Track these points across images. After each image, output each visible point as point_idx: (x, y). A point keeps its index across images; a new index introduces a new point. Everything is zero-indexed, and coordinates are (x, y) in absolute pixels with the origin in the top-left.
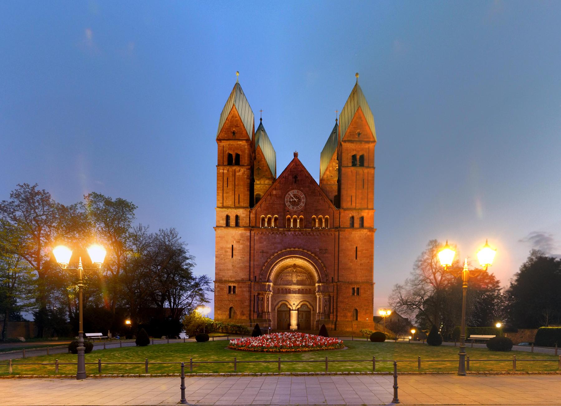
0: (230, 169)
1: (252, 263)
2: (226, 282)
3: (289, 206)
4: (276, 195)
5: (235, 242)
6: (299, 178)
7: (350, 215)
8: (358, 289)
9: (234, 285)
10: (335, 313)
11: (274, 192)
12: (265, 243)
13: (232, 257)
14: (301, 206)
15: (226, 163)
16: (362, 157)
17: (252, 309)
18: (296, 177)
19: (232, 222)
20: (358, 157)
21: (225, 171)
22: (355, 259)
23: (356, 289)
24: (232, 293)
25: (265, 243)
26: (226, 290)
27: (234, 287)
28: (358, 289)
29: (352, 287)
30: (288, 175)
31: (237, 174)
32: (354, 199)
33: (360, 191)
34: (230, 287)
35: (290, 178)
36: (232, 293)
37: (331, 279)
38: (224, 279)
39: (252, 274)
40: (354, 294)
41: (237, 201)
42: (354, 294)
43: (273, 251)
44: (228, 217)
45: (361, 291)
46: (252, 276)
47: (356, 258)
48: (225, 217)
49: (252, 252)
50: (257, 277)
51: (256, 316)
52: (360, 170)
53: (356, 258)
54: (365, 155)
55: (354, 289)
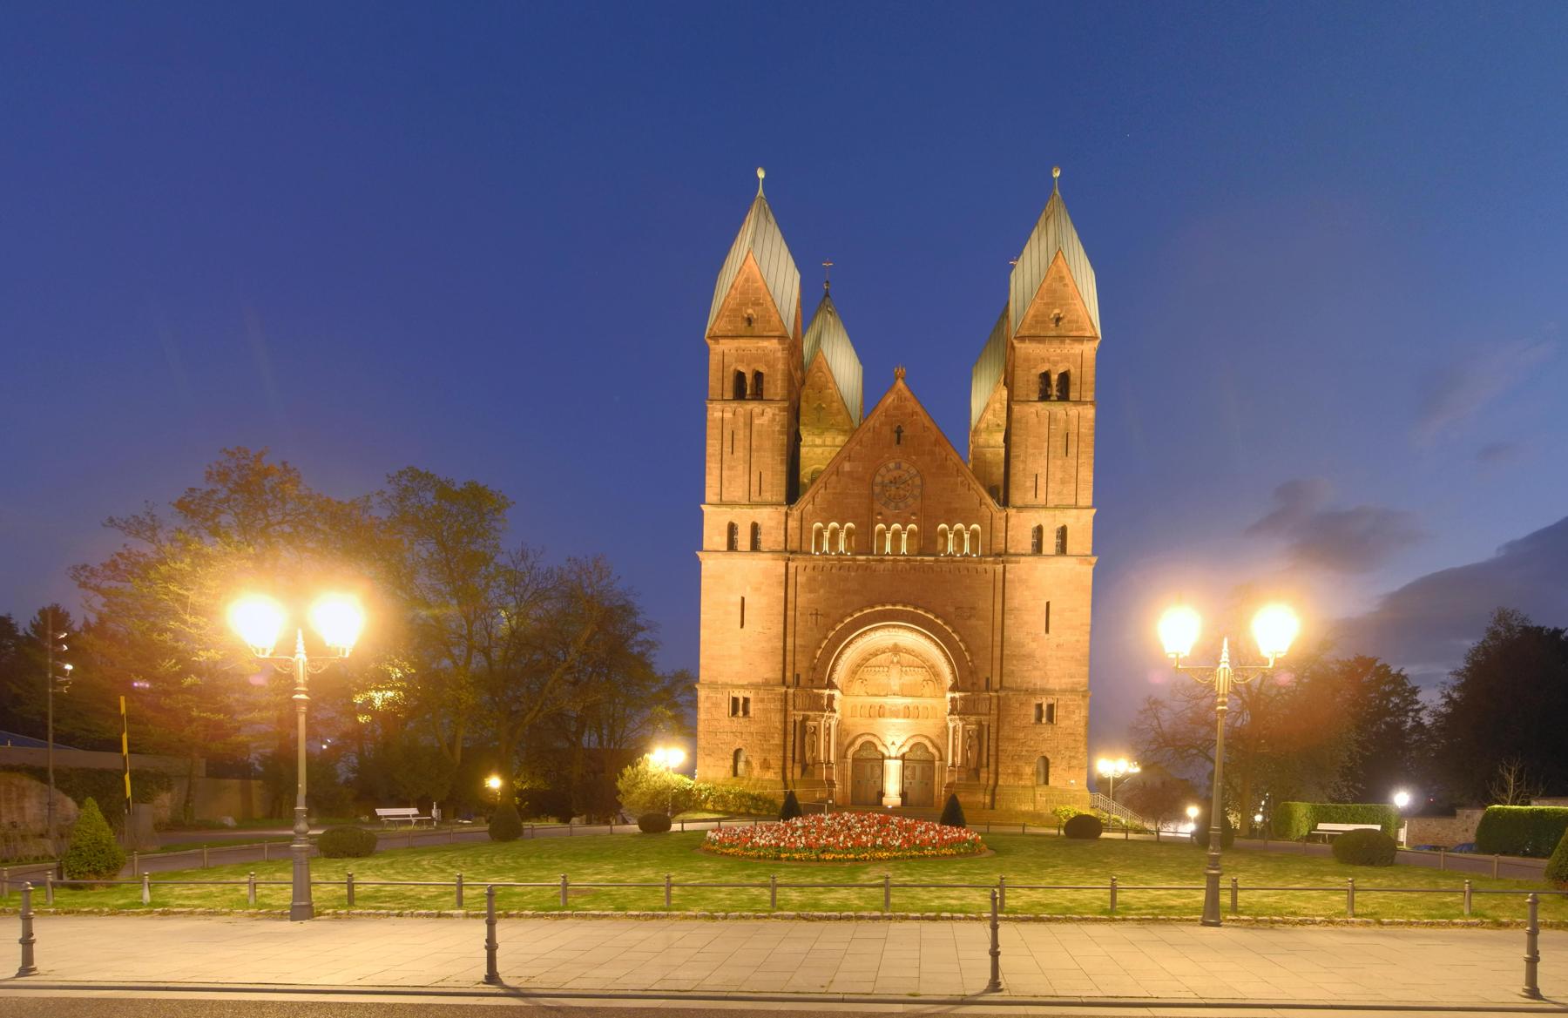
0: (740, 410)
1: (790, 640)
2: (725, 685)
4: (850, 474)
6: (906, 433)
7: (1035, 525)
8: (1051, 707)
10: (992, 767)
11: (847, 466)
15: (729, 395)
16: (1065, 378)
17: (790, 754)
18: (899, 431)
19: (744, 540)
20: (1054, 377)
21: (728, 415)
23: (1045, 707)
24: (741, 713)
26: (726, 707)
27: (746, 700)
28: (1051, 707)
29: (1035, 701)
30: (882, 424)
31: (757, 421)
32: (1042, 481)
33: (1059, 462)
34: (735, 700)
35: (886, 431)
36: (741, 713)
37: (983, 683)
38: (721, 680)
39: (789, 668)
40: (1039, 719)
41: (755, 488)
42: (1039, 719)
44: (732, 529)
45: (1059, 713)
46: (789, 674)
48: (725, 529)
49: (790, 613)
50: (803, 677)
51: (798, 771)
52: (1058, 409)
54: (1072, 371)
55: (1039, 706)
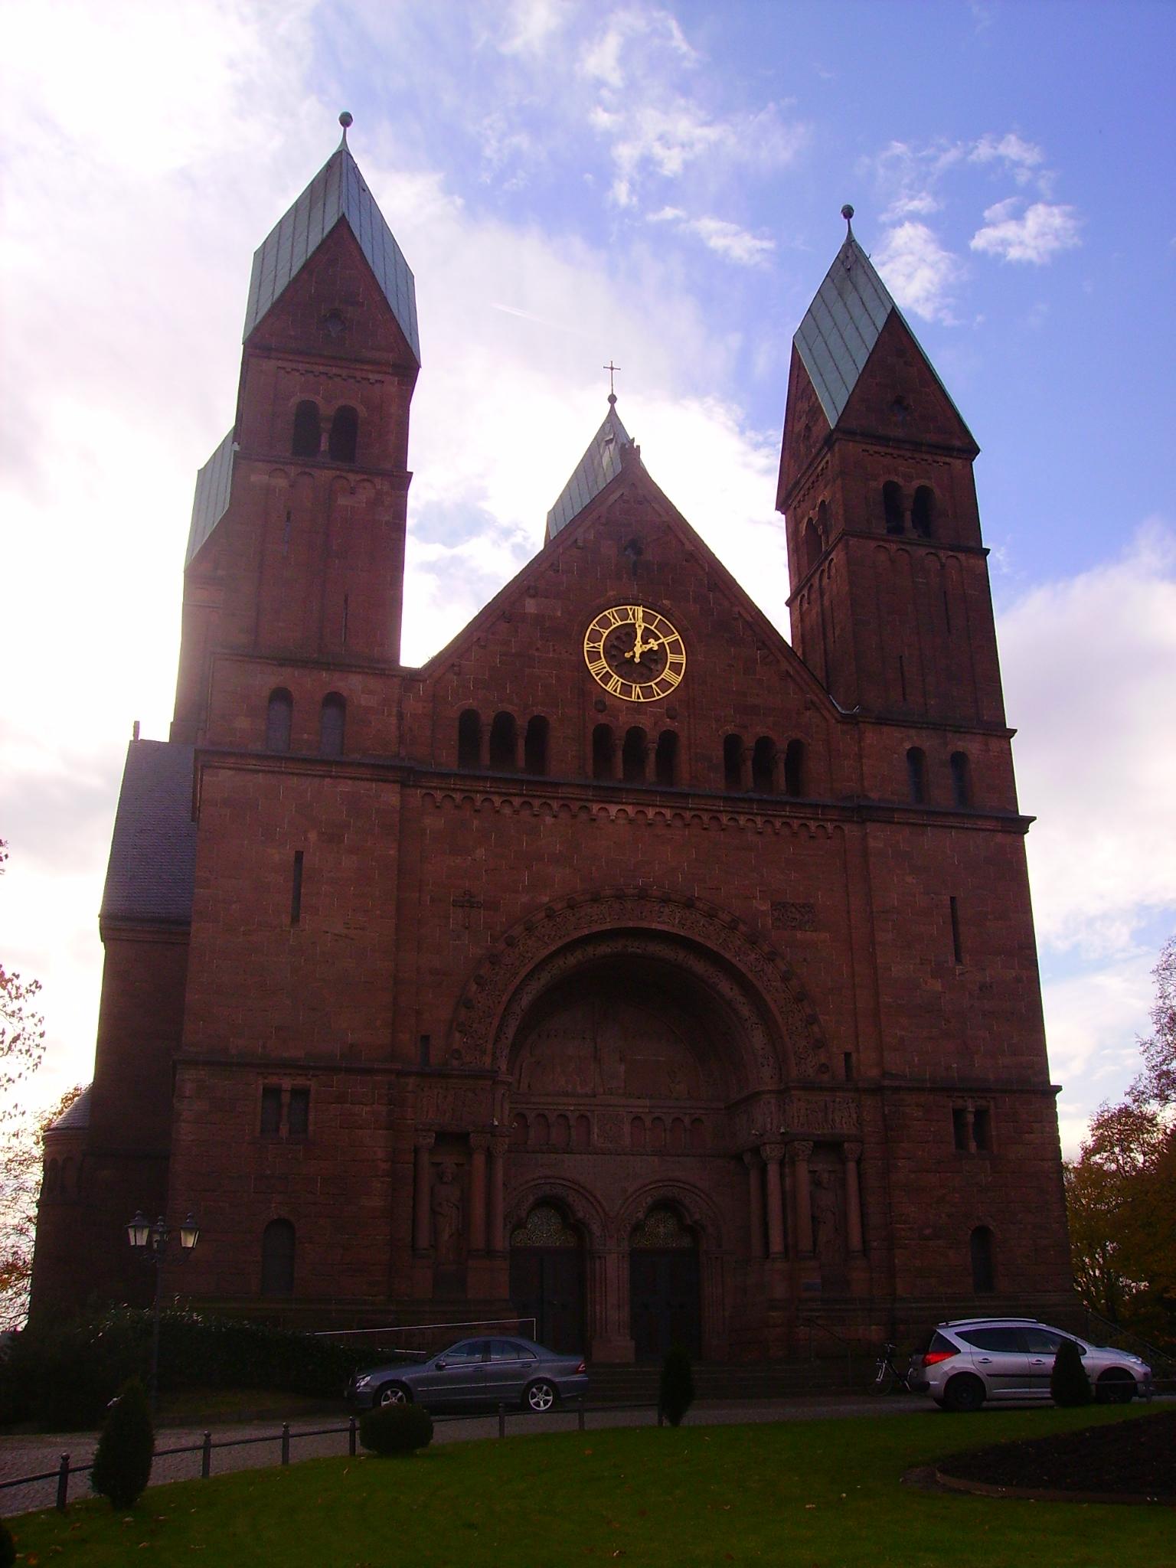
3: (606, 678)
7: (908, 746)
8: (981, 1114)
12: (480, 853)
13: (295, 919)
14: (664, 685)
22: (951, 959)
25: (480, 853)
27: (301, 1093)
28: (981, 1114)
37: (839, 1062)
40: (961, 1144)
42: (961, 1144)
43: (524, 899)
47: (958, 960)
53: (958, 960)
55: (958, 1114)
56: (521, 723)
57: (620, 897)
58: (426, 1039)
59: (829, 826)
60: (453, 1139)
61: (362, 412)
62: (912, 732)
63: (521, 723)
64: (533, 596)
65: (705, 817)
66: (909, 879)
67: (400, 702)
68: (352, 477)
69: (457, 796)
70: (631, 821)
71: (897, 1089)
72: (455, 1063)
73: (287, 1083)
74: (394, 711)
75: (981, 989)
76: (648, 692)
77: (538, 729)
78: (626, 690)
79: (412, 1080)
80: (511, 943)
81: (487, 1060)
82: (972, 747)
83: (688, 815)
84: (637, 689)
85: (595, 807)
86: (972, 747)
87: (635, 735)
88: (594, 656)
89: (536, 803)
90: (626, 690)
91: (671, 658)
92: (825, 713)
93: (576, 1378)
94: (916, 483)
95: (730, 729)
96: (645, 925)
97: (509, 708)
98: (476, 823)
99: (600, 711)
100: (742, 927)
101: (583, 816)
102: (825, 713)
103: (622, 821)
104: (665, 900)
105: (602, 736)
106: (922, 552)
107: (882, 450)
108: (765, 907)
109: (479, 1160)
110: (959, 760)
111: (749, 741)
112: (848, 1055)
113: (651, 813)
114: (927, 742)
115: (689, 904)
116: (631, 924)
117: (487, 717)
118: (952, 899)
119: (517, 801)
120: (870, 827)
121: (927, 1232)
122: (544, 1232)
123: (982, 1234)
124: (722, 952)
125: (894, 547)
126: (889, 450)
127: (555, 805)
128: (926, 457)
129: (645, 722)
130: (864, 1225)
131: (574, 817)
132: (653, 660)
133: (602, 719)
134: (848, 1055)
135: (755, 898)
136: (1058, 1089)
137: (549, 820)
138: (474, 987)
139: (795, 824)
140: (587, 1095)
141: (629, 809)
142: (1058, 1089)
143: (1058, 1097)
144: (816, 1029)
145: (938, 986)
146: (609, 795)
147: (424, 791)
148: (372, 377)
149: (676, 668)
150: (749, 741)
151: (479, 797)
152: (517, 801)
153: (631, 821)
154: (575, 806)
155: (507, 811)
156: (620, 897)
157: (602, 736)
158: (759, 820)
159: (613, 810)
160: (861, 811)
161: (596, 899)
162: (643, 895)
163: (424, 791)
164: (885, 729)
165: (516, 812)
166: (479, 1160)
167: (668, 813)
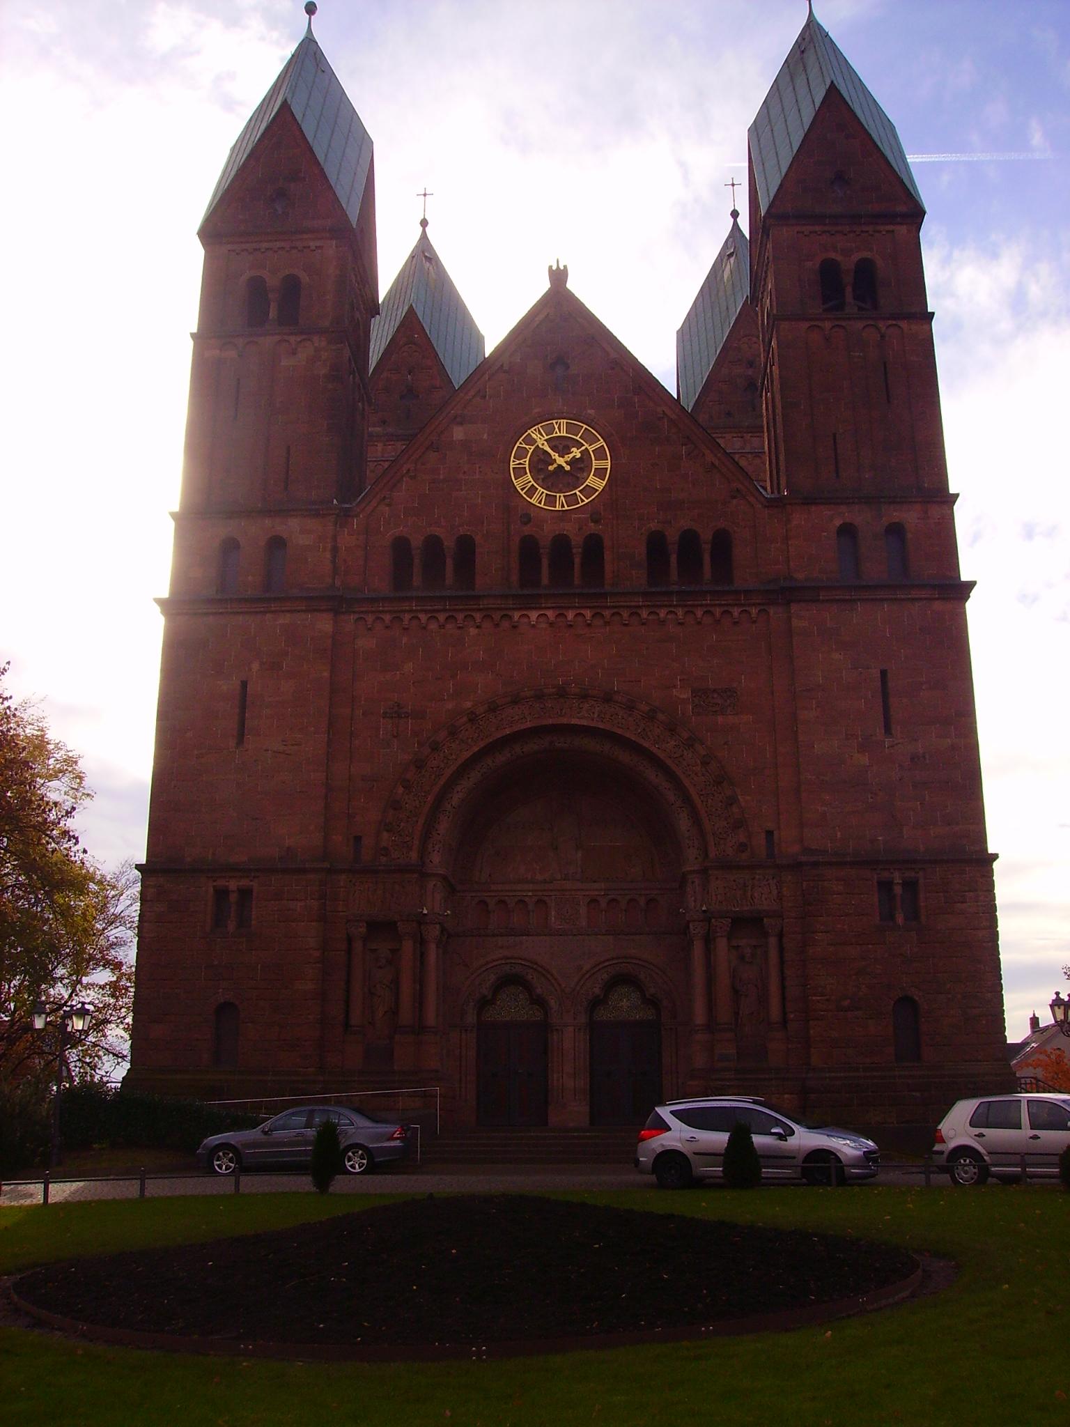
3: (532, 491)
5: (255, 666)
8: (910, 886)
9: (244, 882)
14: (588, 491)
24: (232, 926)
25: (409, 667)
27: (245, 894)
36: (232, 926)
43: (450, 706)
47: (888, 730)
53: (888, 730)
56: (449, 543)
57: (540, 697)
58: (358, 839)
59: (754, 611)
60: (380, 928)
61: (305, 278)
62: (843, 508)
63: (449, 543)
64: (461, 424)
65: (625, 614)
66: (836, 656)
67: (335, 538)
68: (292, 339)
69: (387, 617)
70: (551, 624)
71: (815, 865)
72: (383, 859)
73: (233, 885)
74: (329, 546)
75: (912, 759)
76: (572, 500)
77: (466, 548)
78: (551, 500)
79: (343, 876)
80: (435, 747)
81: (414, 855)
82: (910, 517)
83: (607, 613)
84: (561, 497)
85: (516, 615)
86: (910, 517)
87: (561, 544)
88: (520, 472)
89: (460, 616)
90: (551, 500)
91: (595, 464)
92: (751, 499)
93: (393, 1144)
94: (856, 257)
95: (653, 526)
96: (565, 721)
97: (438, 531)
98: (405, 640)
99: (526, 524)
100: (661, 716)
101: (505, 624)
102: (751, 499)
103: (544, 626)
104: (584, 697)
105: (529, 548)
106: (859, 325)
107: (835, 228)
108: (686, 695)
109: (408, 946)
110: (896, 531)
111: (673, 535)
112: (769, 833)
113: (570, 615)
114: (860, 517)
115: (608, 698)
116: (550, 722)
117: (417, 541)
118: (884, 673)
119: (442, 617)
120: (794, 608)
121: (846, 1003)
122: (512, 1008)
123: (907, 1003)
124: (641, 741)
125: (828, 325)
126: (826, 228)
127: (478, 616)
128: (865, 228)
129: (569, 529)
130: (783, 998)
131: (497, 625)
132: (581, 466)
133: (527, 530)
134: (769, 833)
135: (675, 687)
136: (995, 857)
137: (473, 631)
138: (401, 790)
139: (718, 611)
140: (545, 882)
141: (550, 613)
142: (995, 857)
143: (995, 865)
144: (735, 809)
145: (864, 760)
146: (527, 603)
147: (357, 616)
148: (313, 244)
149: (600, 473)
150: (673, 535)
151: (407, 617)
152: (442, 617)
153: (551, 624)
154: (497, 616)
155: (433, 626)
156: (540, 697)
157: (529, 548)
158: (680, 612)
159: (534, 615)
160: (787, 593)
161: (516, 701)
162: (562, 693)
163: (357, 616)
164: (813, 508)
165: (442, 626)
166: (408, 946)
167: (588, 614)
